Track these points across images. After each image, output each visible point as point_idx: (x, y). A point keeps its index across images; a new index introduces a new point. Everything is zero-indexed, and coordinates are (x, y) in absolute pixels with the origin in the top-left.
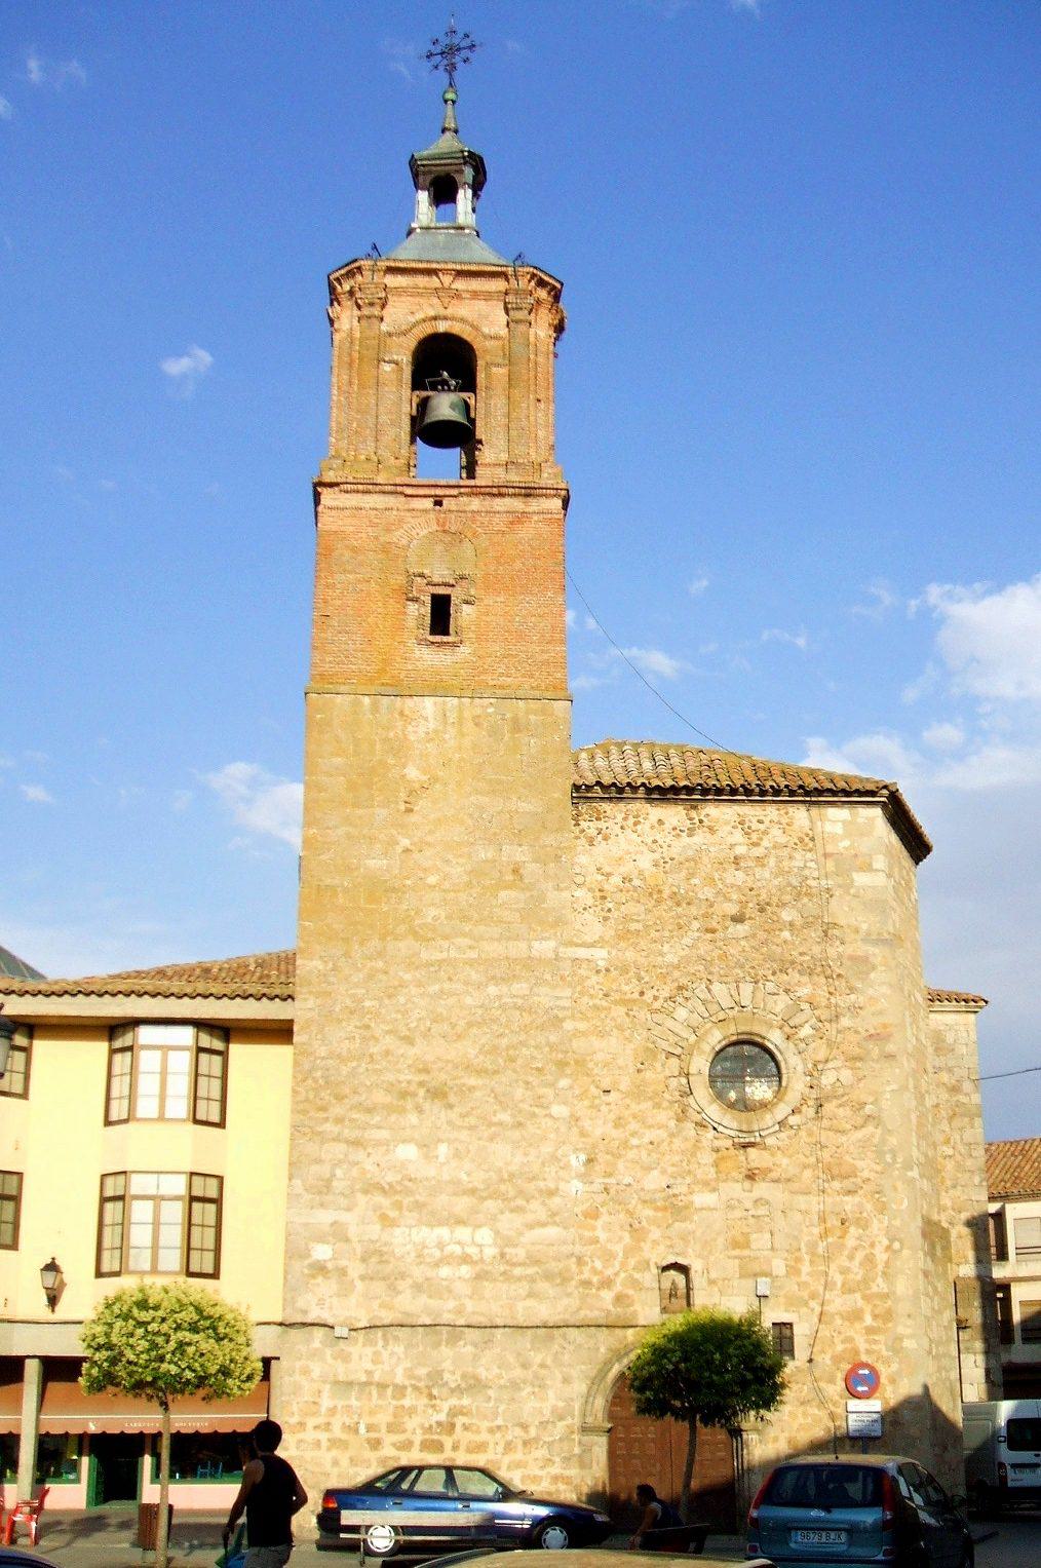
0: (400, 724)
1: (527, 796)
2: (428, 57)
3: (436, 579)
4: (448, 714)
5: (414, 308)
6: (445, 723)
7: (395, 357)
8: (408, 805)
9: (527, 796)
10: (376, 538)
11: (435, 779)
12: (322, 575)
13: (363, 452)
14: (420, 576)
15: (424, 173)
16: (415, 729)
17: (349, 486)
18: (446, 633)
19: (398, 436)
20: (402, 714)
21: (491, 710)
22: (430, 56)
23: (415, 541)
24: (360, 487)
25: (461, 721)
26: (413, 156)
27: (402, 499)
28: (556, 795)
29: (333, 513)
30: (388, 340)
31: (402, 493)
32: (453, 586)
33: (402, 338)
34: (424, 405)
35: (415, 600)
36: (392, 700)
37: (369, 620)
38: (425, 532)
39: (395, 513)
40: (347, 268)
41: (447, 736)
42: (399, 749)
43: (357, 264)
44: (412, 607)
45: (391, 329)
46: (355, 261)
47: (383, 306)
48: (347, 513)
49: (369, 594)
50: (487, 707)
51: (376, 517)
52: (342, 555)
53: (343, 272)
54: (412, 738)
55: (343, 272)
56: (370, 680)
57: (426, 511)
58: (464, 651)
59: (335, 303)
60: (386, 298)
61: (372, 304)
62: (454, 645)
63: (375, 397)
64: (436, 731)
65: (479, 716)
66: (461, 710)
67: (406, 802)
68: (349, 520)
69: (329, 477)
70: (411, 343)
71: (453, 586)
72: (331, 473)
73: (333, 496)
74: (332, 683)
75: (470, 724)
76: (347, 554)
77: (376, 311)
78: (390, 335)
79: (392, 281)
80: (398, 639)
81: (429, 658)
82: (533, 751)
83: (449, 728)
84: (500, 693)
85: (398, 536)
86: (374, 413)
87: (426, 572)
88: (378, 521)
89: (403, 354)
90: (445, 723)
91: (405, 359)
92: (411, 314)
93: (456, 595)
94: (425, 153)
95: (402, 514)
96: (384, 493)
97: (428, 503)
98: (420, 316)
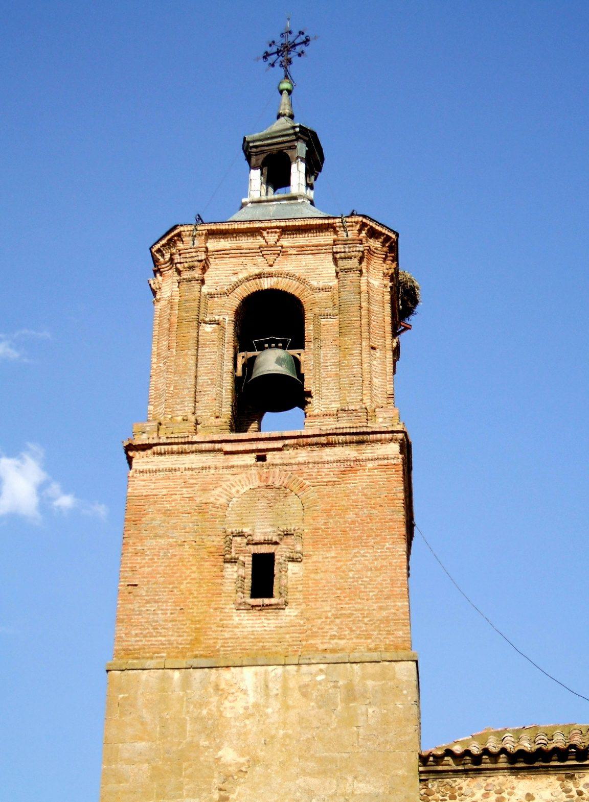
0: (214, 699)
1: (366, 775)
2: (265, 57)
3: (258, 537)
4: (271, 685)
5: (238, 269)
6: (267, 695)
7: (217, 318)
8: (222, 793)
9: (366, 775)
10: (191, 499)
11: (254, 761)
12: (131, 542)
13: (179, 413)
14: (240, 536)
15: (257, 154)
16: (232, 704)
17: (163, 447)
18: (270, 595)
19: (220, 394)
20: (217, 688)
21: (320, 678)
22: (266, 56)
23: (234, 499)
24: (175, 448)
25: (285, 689)
26: (245, 138)
27: (221, 457)
28: (400, 772)
29: (146, 476)
30: (210, 302)
31: (220, 450)
32: (276, 543)
33: (225, 299)
34: (250, 364)
35: (233, 561)
36: (206, 674)
37: (182, 587)
38: (246, 489)
39: (212, 471)
40: (168, 237)
41: (269, 710)
42: (213, 729)
43: (176, 232)
44: (232, 571)
45: (213, 291)
46: (175, 227)
47: (204, 270)
48: (160, 475)
49: (181, 559)
50: (316, 674)
51: (192, 477)
52: (153, 519)
53: (164, 242)
54: (228, 714)
55: (164, 242)
56: (182, 652)
57: (246, 467)
58: (290, 613)
59: (158, 275)
60: (207, 259)
61: (191, 268)
62: (277, 607)
63: (194, 358)
64: (256, 706)
65: (306, 686)
66: (285, 680)
67: (220, 790)
68: (162, 483)
69: (137, 441)
70: (234, 302)
71: (276, 543)
72: (145, 436)
73: (146, 459)
74: (137, 658)
75: (297, 694)
76: (159, 518)
77: (197, 274)
78: (212, 296)
79: (213, 244)
80: (213, 605)
81: (252, 624)
82: (372, 721)
83: (272, 701)
84: (330, 657)
85: (217, 496)
86: (192, 373)
87: (246, 530)
88: (194, 481)
89: (225, 312)
90: (267, 695)
91: (228, 318)
92: (232, 274)
93: (281, 553)
94: (256, 135)
95: (221, 472)
96: (201, 451)
97: (250, 459)
98: (241, 276)
